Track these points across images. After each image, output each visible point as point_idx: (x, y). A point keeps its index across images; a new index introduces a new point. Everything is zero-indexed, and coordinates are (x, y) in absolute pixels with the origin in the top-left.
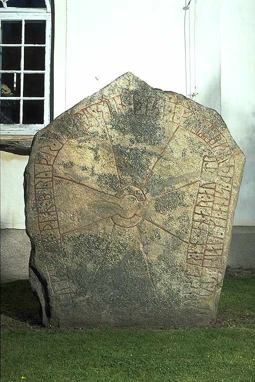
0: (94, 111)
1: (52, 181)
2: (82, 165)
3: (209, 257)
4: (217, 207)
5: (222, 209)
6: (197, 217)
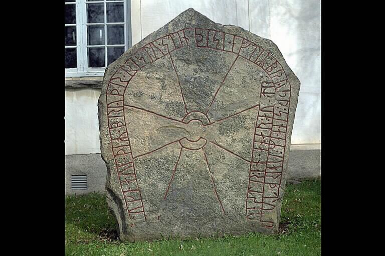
0: (159, 44)
1: (123, 109)
4: (276, 128)
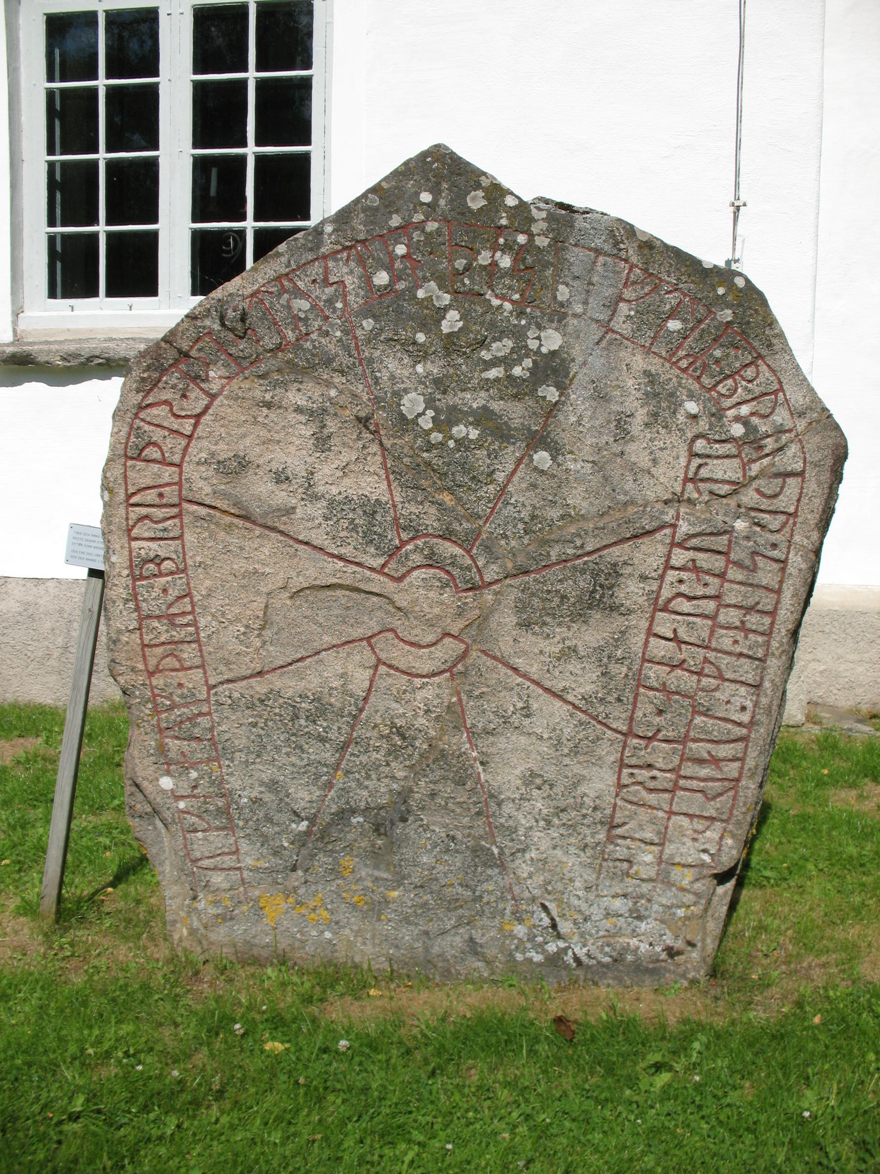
1: (179, 516)
2: (274, 466)
3: (694, 784)
4: (731, 616)
5: (748, 625)
6: (660, 649)
